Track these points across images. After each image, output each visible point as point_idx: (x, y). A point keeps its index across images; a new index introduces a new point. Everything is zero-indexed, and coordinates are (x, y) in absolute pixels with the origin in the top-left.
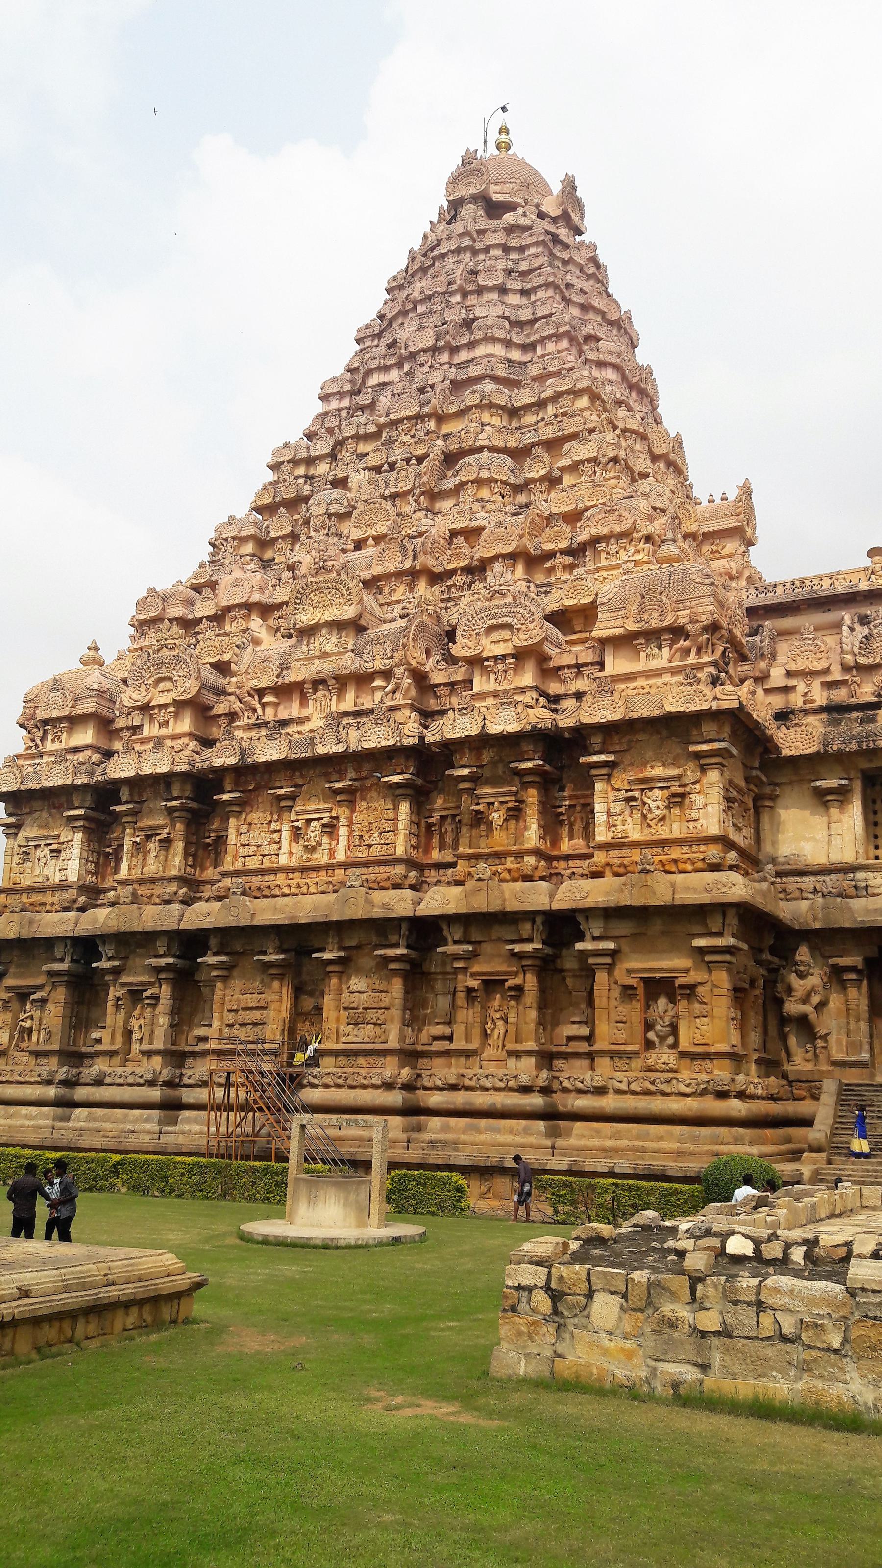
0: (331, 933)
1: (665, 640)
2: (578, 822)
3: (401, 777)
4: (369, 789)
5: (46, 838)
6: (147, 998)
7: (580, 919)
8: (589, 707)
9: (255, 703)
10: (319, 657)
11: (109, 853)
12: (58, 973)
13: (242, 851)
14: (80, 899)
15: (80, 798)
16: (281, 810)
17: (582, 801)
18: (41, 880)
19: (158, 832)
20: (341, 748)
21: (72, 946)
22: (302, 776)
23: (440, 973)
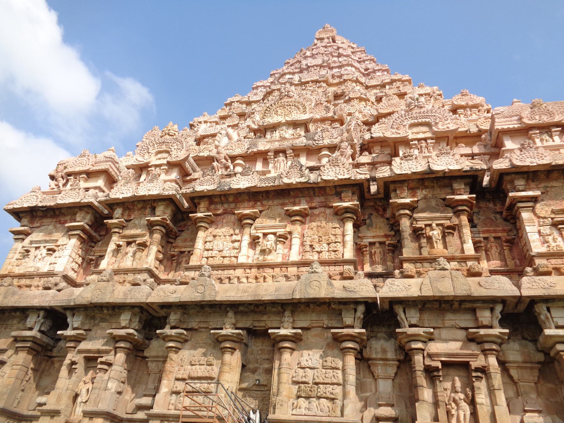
0: (287, 313)
1: (555, 131)
2: (494, 248)
3: (351, 203)
4: (318, 215)
5: (46, 241)
6: (102, 363)
7: (541, 309)
8: (518, 156)
9: (229, 163)
10: (278, 141)
11: (92, 260)
12: (24, 339)
13: (206, 254)
14: (61, 284)
15: (82, 215)
16: (242, 227)
17: (494, 235)
18: (32, 270)
19: (138, 239)
20: (303, 180)
21: (44, 317)
22: (262, 205)
23: (381, 359)
